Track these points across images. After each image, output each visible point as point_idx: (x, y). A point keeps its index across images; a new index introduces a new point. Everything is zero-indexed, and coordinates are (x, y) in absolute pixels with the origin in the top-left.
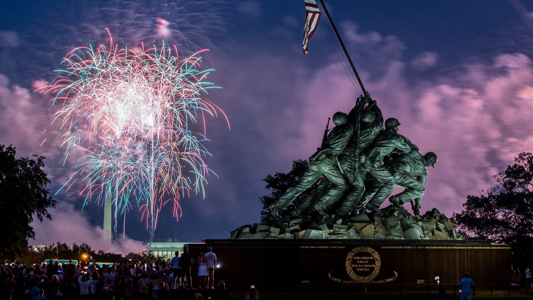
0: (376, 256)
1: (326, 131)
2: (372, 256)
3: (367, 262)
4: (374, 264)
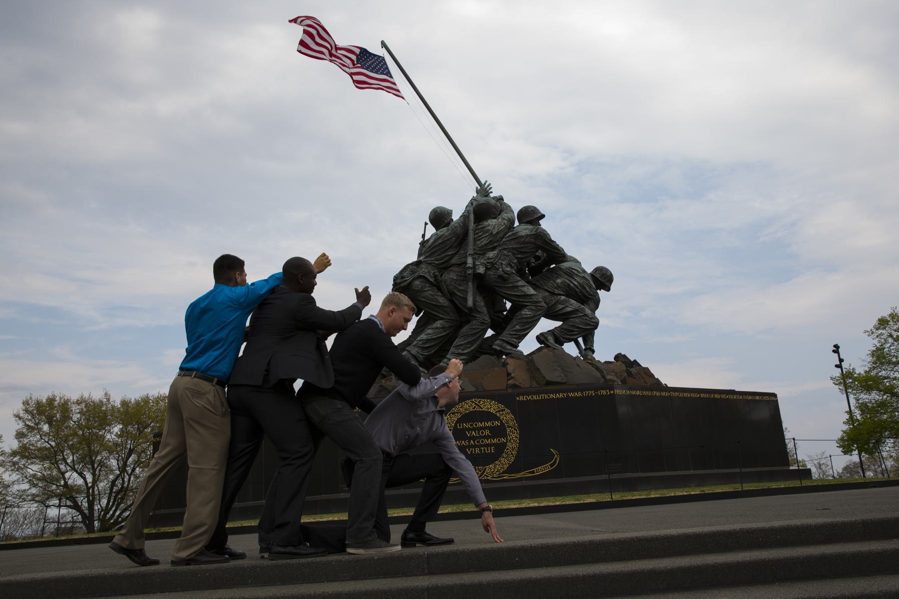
0: (507, 417)
1: (423, 244)
2: (498, 419)
3: (487, 432)
4: (505, 435)
